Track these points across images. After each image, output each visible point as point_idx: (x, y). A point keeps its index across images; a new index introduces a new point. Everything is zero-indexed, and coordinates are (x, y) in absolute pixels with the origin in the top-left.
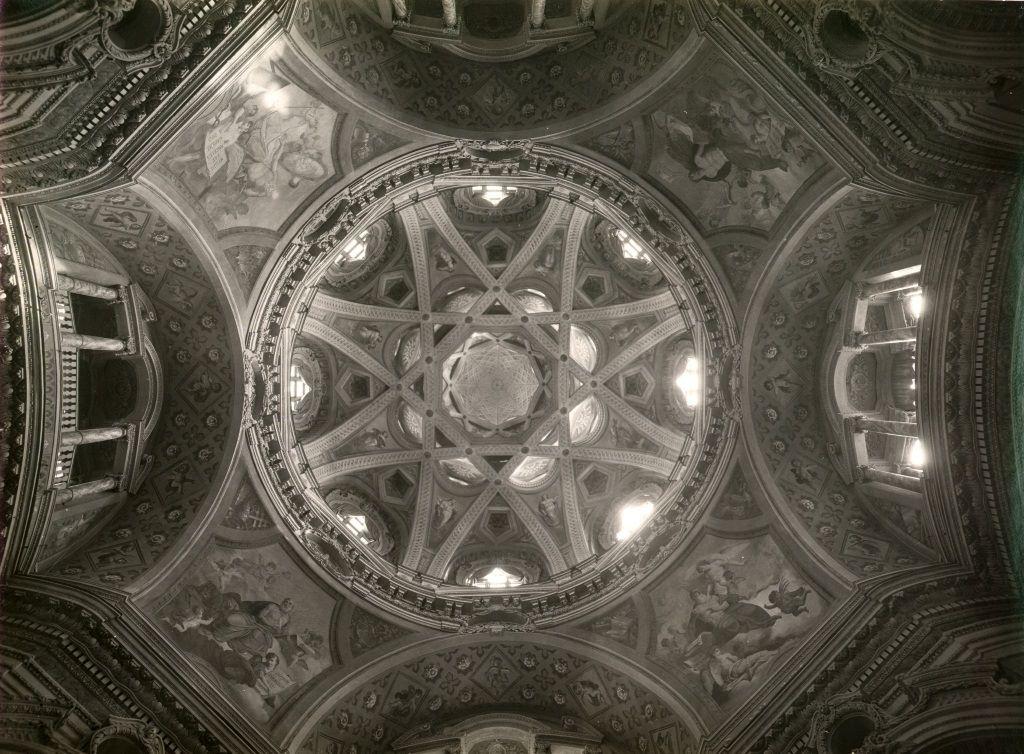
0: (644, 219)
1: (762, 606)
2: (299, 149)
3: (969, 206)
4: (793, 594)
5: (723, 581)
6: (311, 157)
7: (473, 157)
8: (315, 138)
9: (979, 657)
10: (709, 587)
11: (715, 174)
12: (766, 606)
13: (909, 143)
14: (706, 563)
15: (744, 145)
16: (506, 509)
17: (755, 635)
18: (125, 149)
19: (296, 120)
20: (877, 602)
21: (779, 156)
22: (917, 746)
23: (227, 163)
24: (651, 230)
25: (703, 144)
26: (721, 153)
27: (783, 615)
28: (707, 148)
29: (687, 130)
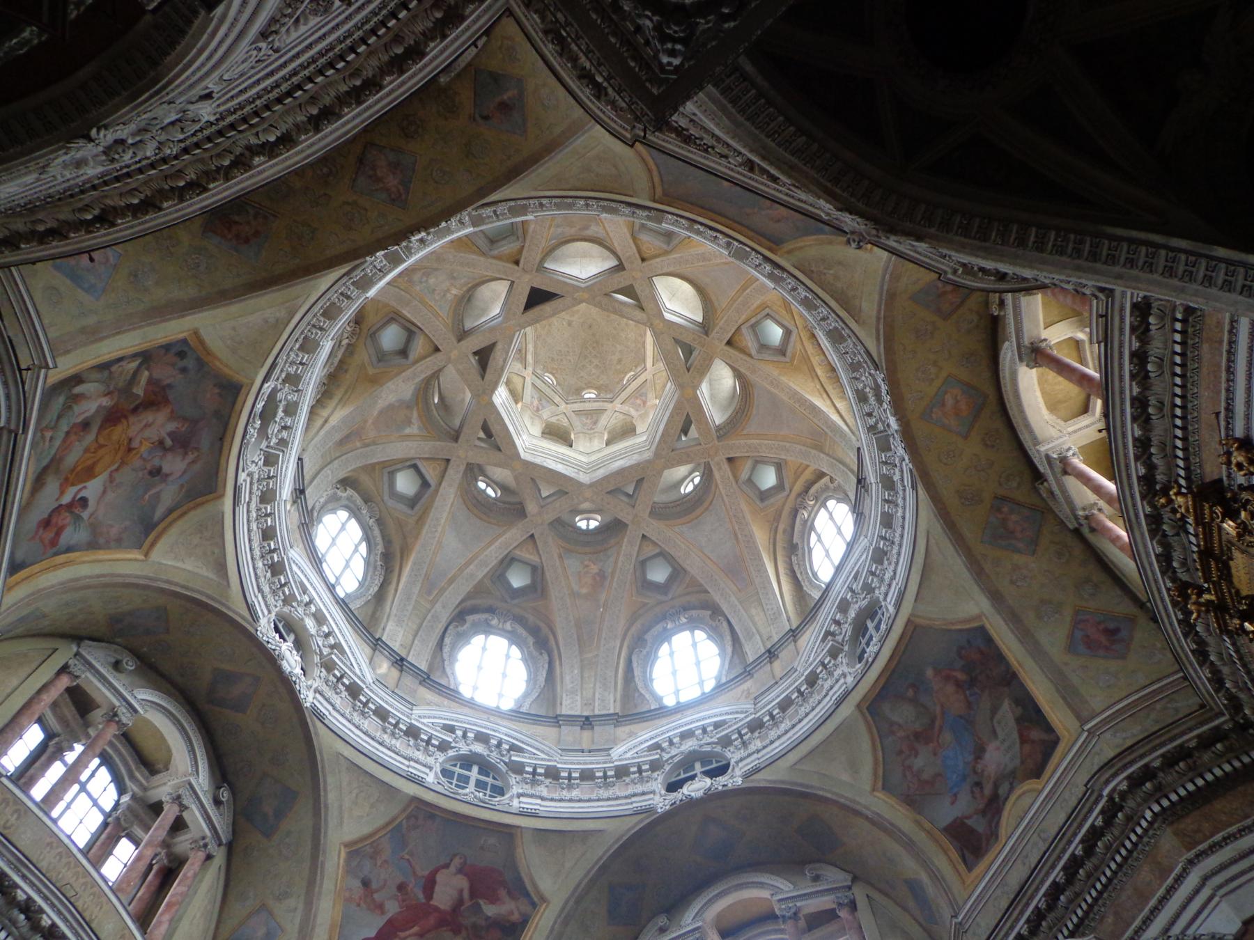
0: (494, 757)
1: (87, 484)
2: (917, 736)
5: (156, 462)
6: (900, 726)
7: (718, 749)
8: (900, 752)
10: (169, 442)
11: (440, 878)
14: (193, 462)
16: (495, 252)
17: (73, 457)
18: (1091, 811)
19: (925, 776)
23: (992, 719)
24: (479, 748)
25: (468, 903)
26: (442, 907)
28: (460, 902)
29: (490, 910)
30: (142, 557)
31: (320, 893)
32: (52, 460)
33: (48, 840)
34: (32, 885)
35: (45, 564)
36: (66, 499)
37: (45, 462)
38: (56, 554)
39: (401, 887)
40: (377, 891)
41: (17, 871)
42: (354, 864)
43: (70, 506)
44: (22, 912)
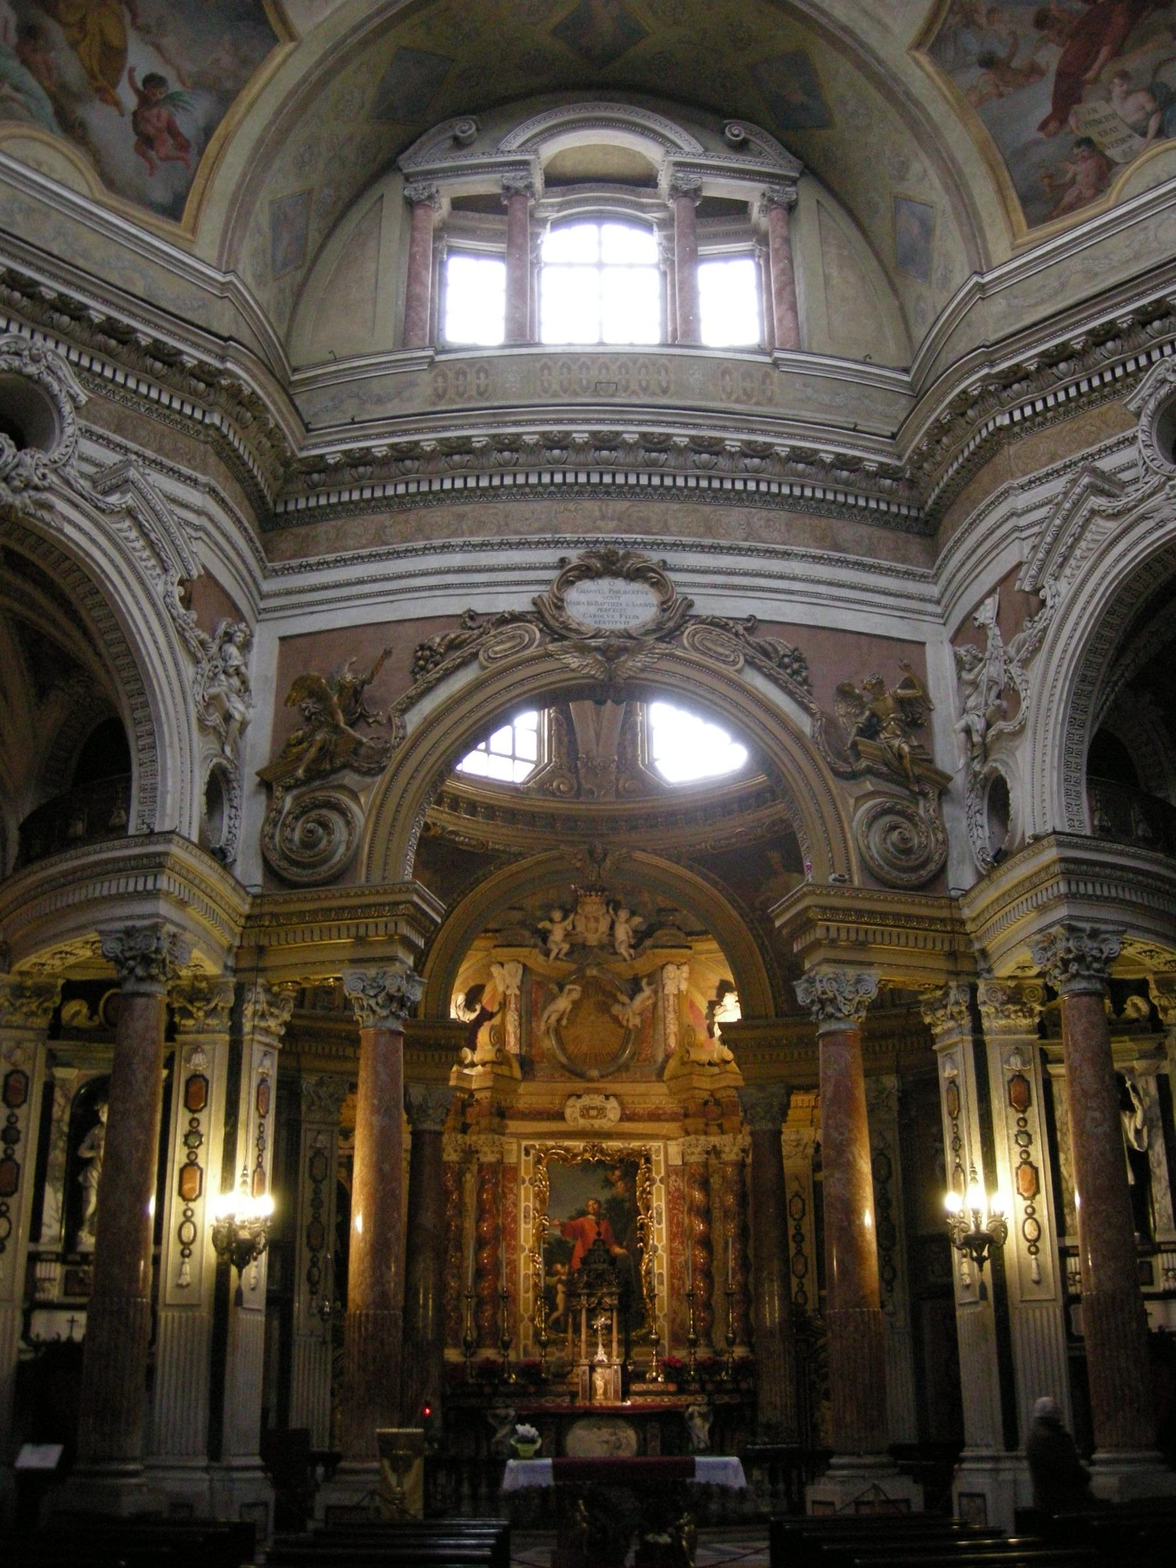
1: (128, 66)
3: (889, 454)
4: (172, 129)
9: (194, 534)
12: (132, 70)
13: (1007, 421)
15: (1117, 53)
17: (71, 68)
20: (223, 359)
21: (1072, 121)
22: (61, 531)
27: (128, 119)
30: (291, 46)
31: (935, 127)
32: (53, 98)
33: (538, 365)
34: (532, 422)
35: (203, 171)
36: (130, 101)
37: (49, 108)
38: (201, 152)
39: (1041, 21)
40: (1012, 55)
41: (505, 424)
42: (950, 54)
43: (145, 100)
44: (551, 449)
